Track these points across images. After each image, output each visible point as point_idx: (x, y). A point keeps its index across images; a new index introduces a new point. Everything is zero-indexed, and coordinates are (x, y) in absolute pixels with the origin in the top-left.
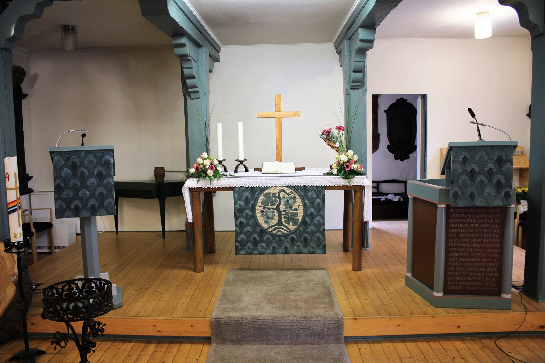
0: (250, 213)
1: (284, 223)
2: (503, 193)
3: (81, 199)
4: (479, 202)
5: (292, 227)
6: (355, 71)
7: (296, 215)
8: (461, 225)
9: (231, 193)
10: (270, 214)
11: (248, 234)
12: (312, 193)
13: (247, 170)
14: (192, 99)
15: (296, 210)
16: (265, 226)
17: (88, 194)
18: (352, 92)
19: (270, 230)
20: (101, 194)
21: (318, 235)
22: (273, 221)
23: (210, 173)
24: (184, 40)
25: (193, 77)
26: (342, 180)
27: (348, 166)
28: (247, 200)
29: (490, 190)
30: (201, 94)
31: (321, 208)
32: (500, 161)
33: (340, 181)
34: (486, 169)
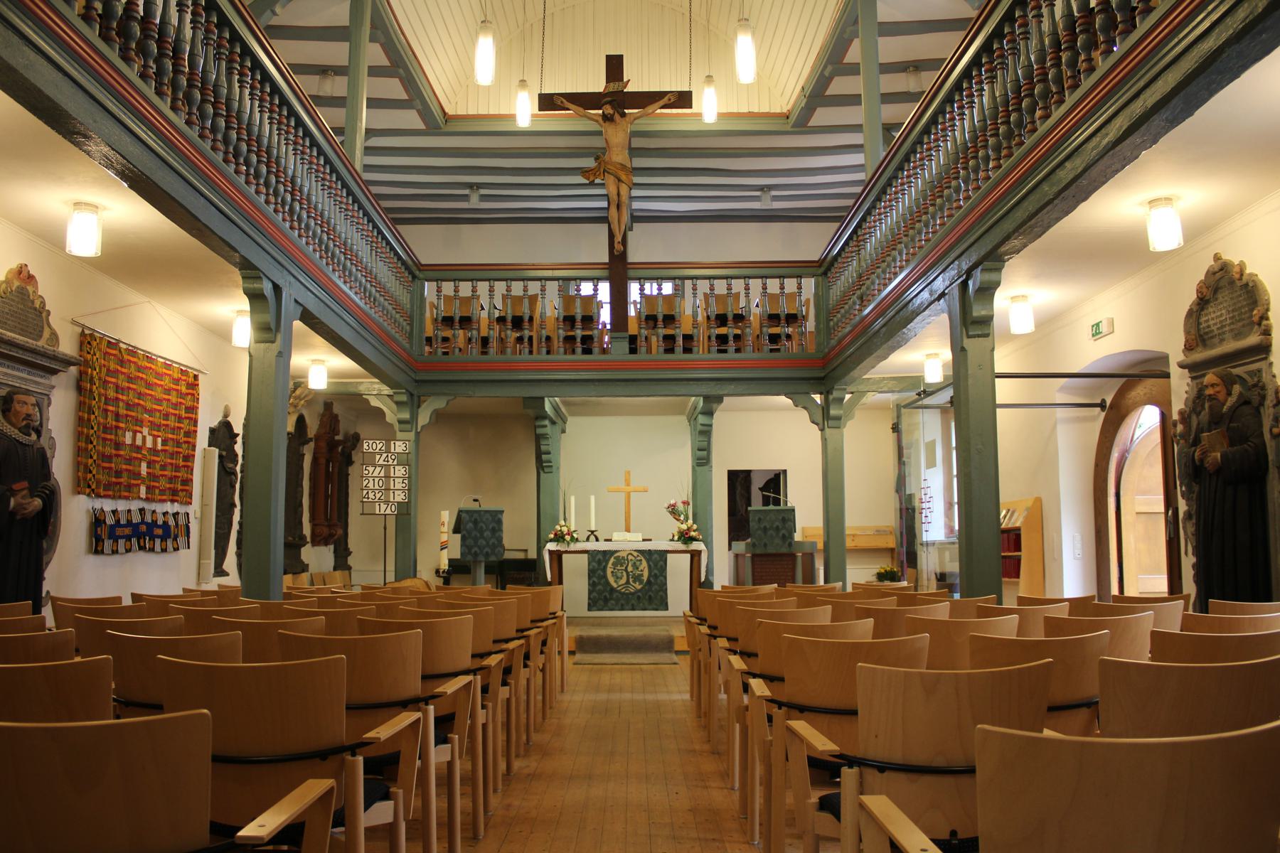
0: (602, 574)
1: (631, 583)
2: (787, 543)
3: (479, 547)
4: (771, 550)
5: (638, 586)
6: (699, 450)
7: (642, 575)
9: (586, 555)
10: (619, 575)
11: (600, 593)
12: (656, 556)
13: (597, 540)
14: (544, 472)
15: (642, 571)
16: (615, 585)
17: (484, 543)
18: (697, 468)
19: (619, 589)
20: (493, 543)
21: (661, 593)
23: (568, 538)
24: (547, 422)
25: (549, 453)
26: (682, 545)
27: (687, 534)
28: (599, 562)
29: (778, 541)
30: (554, 469)
31: (663, 569)
32: (784, 520)
33: (680, 546)
34: (775, 526)
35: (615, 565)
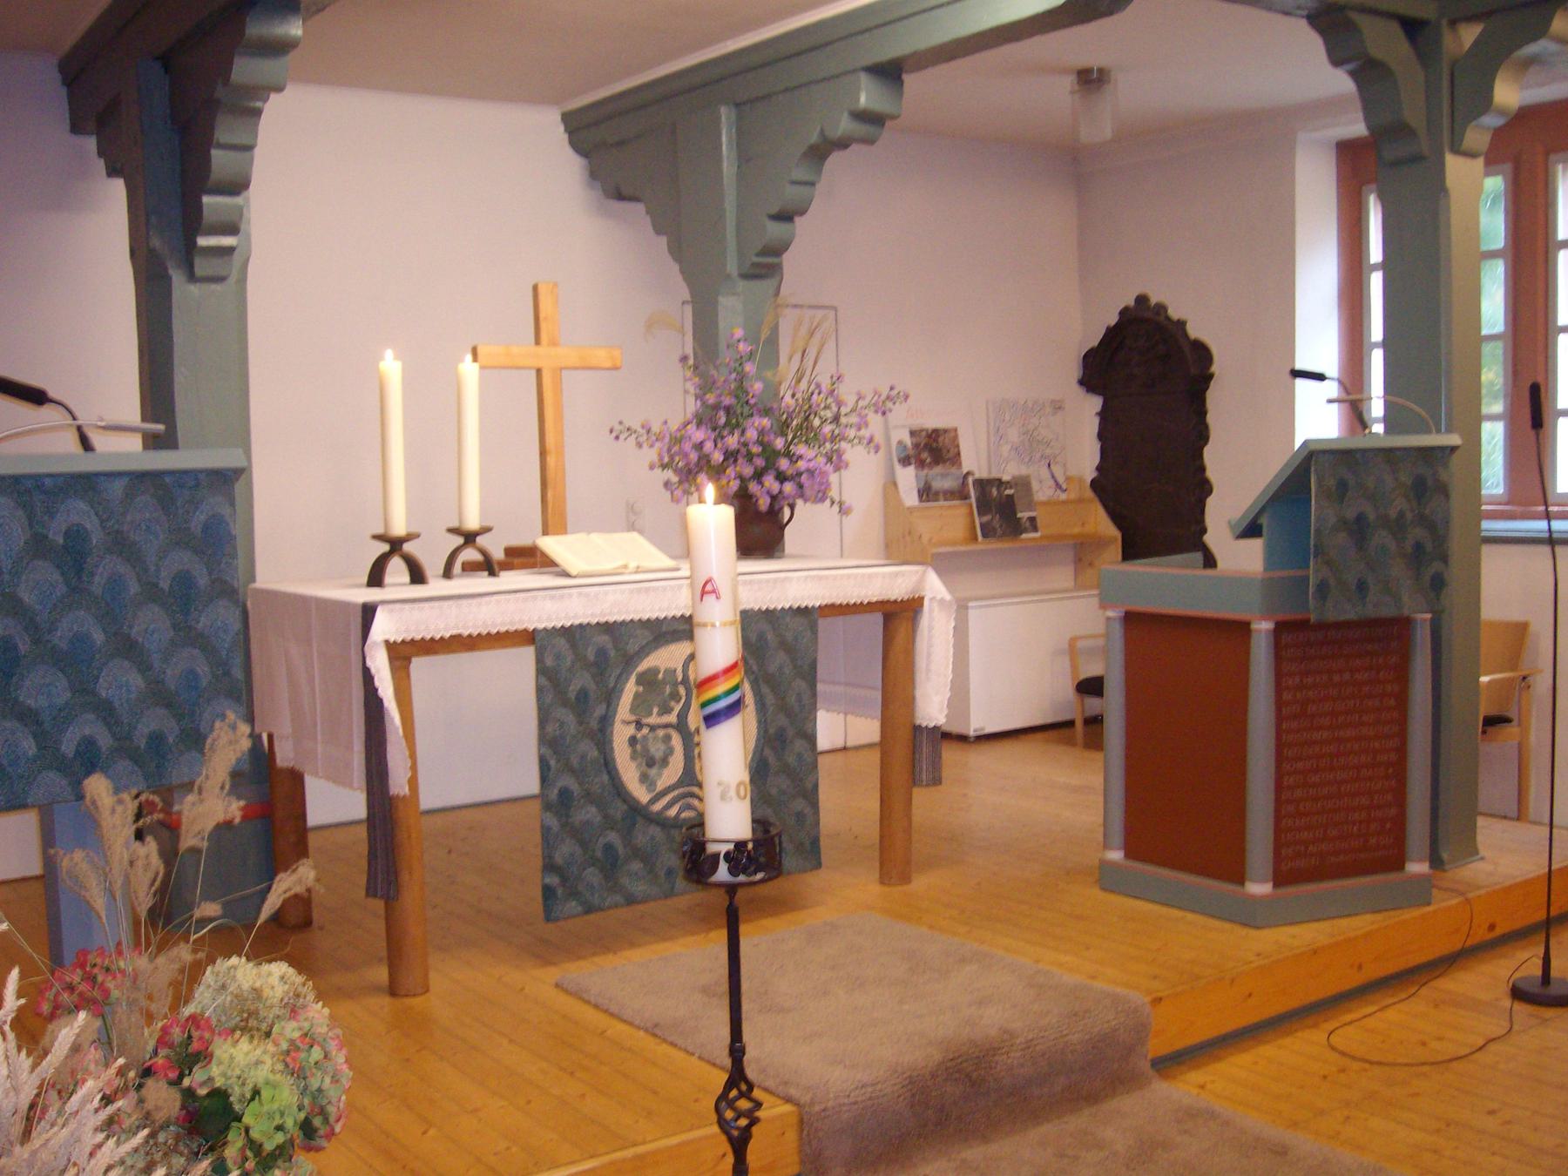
8: (1310, 680)
10: (657, 750)
16: (642, 795)
19: (657, 807)
22: (666, 772)
25: (232, 229)
35: (639, 704)
